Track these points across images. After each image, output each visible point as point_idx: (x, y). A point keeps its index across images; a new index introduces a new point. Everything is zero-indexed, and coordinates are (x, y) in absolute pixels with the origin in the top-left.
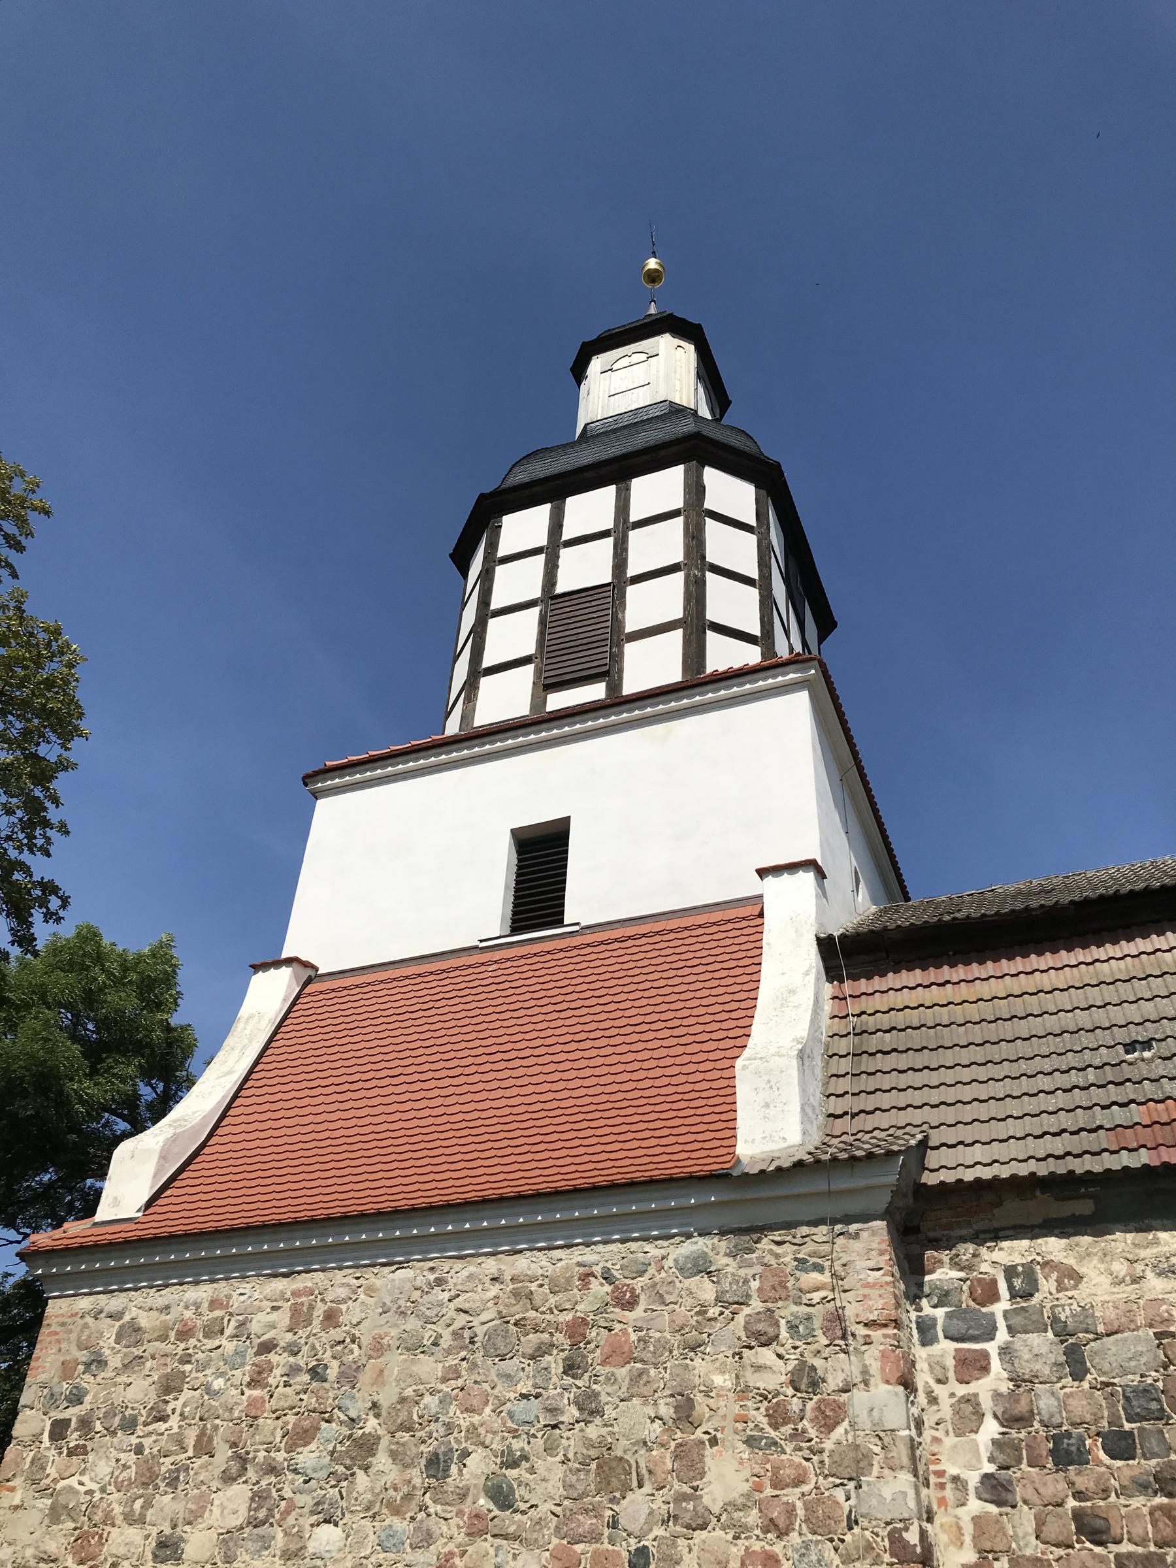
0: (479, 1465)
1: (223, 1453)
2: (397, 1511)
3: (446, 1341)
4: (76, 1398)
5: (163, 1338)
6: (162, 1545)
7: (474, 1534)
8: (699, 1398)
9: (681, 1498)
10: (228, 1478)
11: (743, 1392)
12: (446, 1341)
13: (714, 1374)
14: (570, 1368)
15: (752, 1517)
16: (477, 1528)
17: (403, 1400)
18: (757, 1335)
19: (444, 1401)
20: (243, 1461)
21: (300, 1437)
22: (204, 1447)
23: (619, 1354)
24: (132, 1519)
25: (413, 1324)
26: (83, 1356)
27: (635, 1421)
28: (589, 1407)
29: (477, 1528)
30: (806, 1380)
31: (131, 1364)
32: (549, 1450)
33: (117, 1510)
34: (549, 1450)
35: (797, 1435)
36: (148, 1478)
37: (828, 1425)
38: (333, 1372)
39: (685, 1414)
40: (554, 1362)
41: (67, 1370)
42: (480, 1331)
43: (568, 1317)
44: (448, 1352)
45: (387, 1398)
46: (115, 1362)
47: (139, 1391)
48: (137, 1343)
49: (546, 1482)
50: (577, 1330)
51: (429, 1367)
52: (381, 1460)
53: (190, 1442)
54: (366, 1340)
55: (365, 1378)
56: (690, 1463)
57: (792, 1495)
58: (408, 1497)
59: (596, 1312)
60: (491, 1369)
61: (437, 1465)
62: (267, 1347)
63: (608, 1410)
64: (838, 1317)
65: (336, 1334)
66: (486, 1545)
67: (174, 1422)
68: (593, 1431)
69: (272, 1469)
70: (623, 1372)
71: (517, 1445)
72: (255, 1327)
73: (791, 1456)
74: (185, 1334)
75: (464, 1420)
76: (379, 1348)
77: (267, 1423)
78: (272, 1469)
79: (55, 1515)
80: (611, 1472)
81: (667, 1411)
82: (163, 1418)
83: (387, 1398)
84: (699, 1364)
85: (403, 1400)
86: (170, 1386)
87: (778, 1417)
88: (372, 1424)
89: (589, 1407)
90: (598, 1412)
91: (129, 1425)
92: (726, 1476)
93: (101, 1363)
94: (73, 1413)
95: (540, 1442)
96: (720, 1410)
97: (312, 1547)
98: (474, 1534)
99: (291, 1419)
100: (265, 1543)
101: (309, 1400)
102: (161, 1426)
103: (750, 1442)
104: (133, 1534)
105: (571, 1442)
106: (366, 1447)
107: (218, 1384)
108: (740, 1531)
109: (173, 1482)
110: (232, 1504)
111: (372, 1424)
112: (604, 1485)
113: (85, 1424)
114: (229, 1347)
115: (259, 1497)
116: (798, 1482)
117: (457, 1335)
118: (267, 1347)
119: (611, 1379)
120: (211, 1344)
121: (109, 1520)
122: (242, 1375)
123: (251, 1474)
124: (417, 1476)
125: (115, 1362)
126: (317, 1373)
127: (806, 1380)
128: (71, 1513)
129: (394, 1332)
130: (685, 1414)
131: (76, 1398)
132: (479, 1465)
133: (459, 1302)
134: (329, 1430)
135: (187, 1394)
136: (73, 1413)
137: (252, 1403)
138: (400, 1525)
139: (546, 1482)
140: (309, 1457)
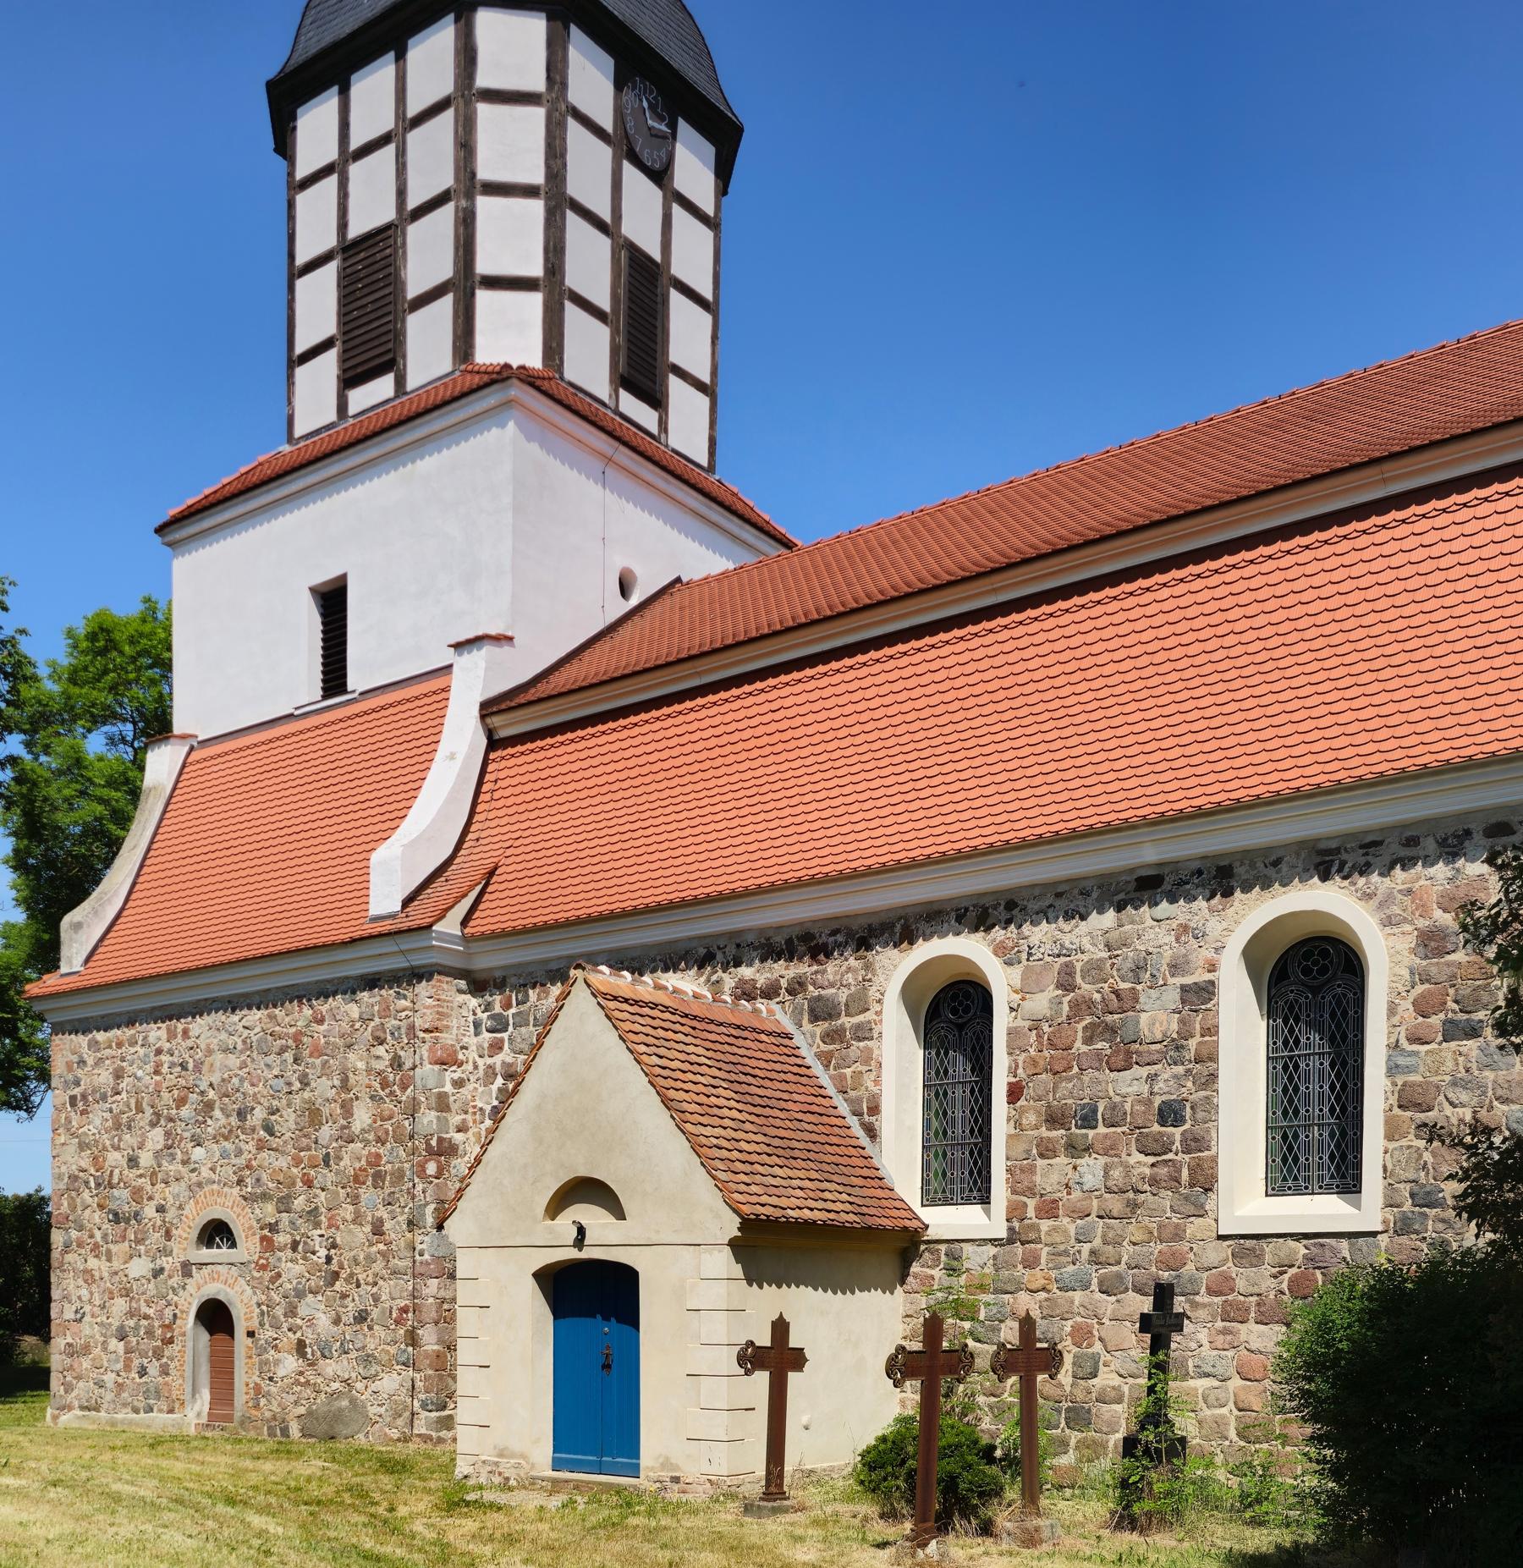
0: (259, 1114)
1: (149, 1111)
2: (226, 1139)
3: (240, 1046)
4: (77, 1083)
5: (110, 1047)
6: (130, 1160)
7: (260, 1149)
8: (351, 1075)
9: (343, 1127)
10: (153, 1125)
11: (369, 1071)
12: (240, 1046)
13: (357, 1061)
14: (296, 1061)
15: (371, 1137)
16: (261, 1146)
17: (223, 1080)
18: (377, 1038)
19: (242, 1080)
20: (158, 1115)
21: (181, 1102)
22: (140, 1109)
23: (317, 1052)
24: (117, 1148)
25: (224, 1036)
26: (75, 1058)
27: (324, 1088)
28: (305, 1083)
29: (261, 1146)
30: (397, 1063)
31: (99, 1062)
32: (289, 1105)
33: (108, 1143)
34: (289, 1105)
35: (392, 1093)
36: (117, 1126)
37: (404, 1088)
38: (191, 1066)
39: (345, 1085)
40: (289, 1056)
41: (69, 1066)
42: (254, 1039)
43: (293, 1030)
44: (242, 1052)
45: (216, 1079)
46: (90, 1062)
47: (104, 1077)
48: (99, 1050)
49: (288, 1121)
50: (297, 1038)
51: (233, 1061)
52: (217, 1113)
53: (133, 1106)
54: (203, 1046)
55: (205, 1069)
56: (347, 1111)
57: (388, 1126)
58: (231, 1131)
59: (307, 1026)
60: (262, 1061)
61: (242, 1115)
62: (159, 1052)
63: (313, 1084)
64: (412, 1027)
65: (190, 1043)
66: (265, 1154)
67: (124, 1095)
68: (306, 1095)
69: (171, 1120)
70: (318, 1062)
71: (275, 1103)
72: (151, 1039)
73: (389, 1105)
74: (120, 1045)
75: (251, 1090)
76: (209, 1052)
77: (165, 1095)
78: (171, 1120)
79: (82, 1146)
80: (314, 1116)
81: (337, 1083)
82: (118, 1093)
83: (216, 1079)
84: (351, 1056)
85: (223, 1080)
86: (118, 1075)
87: (385, 1084)
88: (211, 1094)
89: (305, 1083)
90: (307, 1084)
91: (104, 1098)
92: (362, 1116)
93: (84, 1062)
94: (77, 1091)
95: (284, 1101)
96: (359, 1080)
97: (193, 1158)
98: (260, 1149)
99: (176, 1092)
100: (173, 1157)
101: (183, 1082)
102: (118, 1097)
103: (372, 1098)
104: (117, 1155)
105: (297, 1100)
106: (209, 1106)
107: (140, 1073)
108: (367, 1143)
109: (129, 1128)
110: (156, 1137)
111: (211, 1094)
112: (312, 1123)
113: (84, 1097)
114: (142, 1051)
115: (168, 1134)
116: (390, 1118)
117: (244, 1042)
118: (159, 1052)
119: (314, 1066)
120: (133, 1050)
121: (105, 1149)
122: (150, 1068)
123: (162, 1122)
124: (234, 1120)
125: (90, 1062)
126: (184, 1067)
127: (397, 1063)
128: (88, 1146)
129: (215, 1041)
130: (345, 1085)
131: (77, 1083)
132: (259, 1114)
133: (244, 1022)
134: (193, 1097)
135: (127, 1080)
136: (77, 1091)
137: (157, 1083)
138: (227, 1145)
139: (288, 1121)
140: (185, 1112)
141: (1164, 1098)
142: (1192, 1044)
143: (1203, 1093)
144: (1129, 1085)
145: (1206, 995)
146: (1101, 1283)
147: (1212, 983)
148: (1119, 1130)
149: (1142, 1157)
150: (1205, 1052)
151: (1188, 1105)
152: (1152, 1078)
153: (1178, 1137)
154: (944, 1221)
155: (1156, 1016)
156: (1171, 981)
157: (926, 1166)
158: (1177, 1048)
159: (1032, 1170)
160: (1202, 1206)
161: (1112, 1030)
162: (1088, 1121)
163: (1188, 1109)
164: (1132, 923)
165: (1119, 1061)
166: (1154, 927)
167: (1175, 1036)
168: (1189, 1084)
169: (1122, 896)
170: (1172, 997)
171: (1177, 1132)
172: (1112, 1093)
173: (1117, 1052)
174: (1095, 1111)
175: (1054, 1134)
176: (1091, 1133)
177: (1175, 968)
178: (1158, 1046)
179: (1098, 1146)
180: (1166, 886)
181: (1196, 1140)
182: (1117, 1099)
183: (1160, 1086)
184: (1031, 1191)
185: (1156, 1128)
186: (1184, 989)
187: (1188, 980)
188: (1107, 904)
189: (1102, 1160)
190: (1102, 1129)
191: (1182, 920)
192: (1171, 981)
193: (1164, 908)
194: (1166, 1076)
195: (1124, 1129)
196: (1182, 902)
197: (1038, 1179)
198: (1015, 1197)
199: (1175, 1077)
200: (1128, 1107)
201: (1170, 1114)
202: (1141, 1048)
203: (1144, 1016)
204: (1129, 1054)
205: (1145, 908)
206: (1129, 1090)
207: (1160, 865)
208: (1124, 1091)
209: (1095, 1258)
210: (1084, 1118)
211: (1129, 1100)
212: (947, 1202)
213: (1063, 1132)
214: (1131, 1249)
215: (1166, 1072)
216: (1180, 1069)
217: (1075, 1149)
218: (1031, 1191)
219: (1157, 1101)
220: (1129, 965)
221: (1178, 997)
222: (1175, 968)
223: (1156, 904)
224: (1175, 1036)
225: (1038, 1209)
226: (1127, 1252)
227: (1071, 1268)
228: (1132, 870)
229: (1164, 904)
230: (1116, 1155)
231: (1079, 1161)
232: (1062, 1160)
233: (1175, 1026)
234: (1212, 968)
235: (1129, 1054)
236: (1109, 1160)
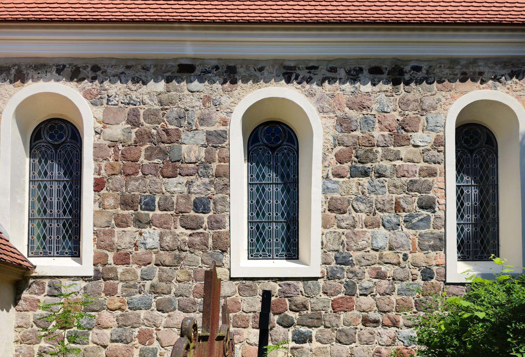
141: (197, 196)
142: (214, 166)
143: (220, 195)
144: (176, 186)
145: (221, 138)
146: (158, 305)
147: (225, 132)
148: (169, 213)
149: (183, 230)
150: (221, 171)
151: (212, 201)
152: (189, 184)
153: (206, 220)
154: (45, 265)
155: (191, 148)
156: (200, 128)
157: (31, 232)
158: (205, 168)
159: (112, 233)
160: (221, 260)
161: (165, 153)
162: (149, 206)
163: (212, 204)
164: (176, 90)
165: (168, 171)
166: (191, 94)
167: (203, 160)
168: (212, 189)
169: (169, 74)
170: (201, 138)
171: (205, 217)
172: (164, 190)
173: (168, 166)
174: (154, 201)
175: (126, 212)
176: (151, 214)
177: (203, 120)
178: (193, 165)
179: (156, 222)
180: (197, 72)
181: (217, 222)
182: (168, 194)
183: (194, 189)
184: (110, 247)
185: (192, 213)
186: (209, 133)
187: (211, 129)
188: (160, 78)
189: (158, 230)
190: (158, 212)
191: (206, 93)
192: (200, 128)
193: (196, 85)
194: (198, 183)
195: (172, 212)
196: (206, 83)
197: (116, 240)
198: (99, 250)
199: (204, 184)
200: (174, 199)
201: (201, 206)
202: (182, 165)
203: (183, 146)
204: (175, 168)
205: (184, 83)
206: (176, 189)
207: (194, 59)
208: (173, 189)
209: (154, 290)
210: (146, 204)
211: (175, 195)
212: (46, 255)
213: (133, 211)
214: (177, 284)
215: (199, 182)
216: (207, 180)
217: (140, 223)
218: (110, 247)
219: (193, 197)
220: (174, 115)
221: (205, 138)
222: (203, 120)
223: (191, 82)
224: (203, 160)
225: (115, 258)
226: (174, 287)
227: (138, 296)
228: (176, 59)
229: (196, 83)
230: (167, 228)
231: (143, 230)
232: (132, 229)
233: (203, 154)
234: (225, 123)
235: (175, 168)
236: (163, 230)
